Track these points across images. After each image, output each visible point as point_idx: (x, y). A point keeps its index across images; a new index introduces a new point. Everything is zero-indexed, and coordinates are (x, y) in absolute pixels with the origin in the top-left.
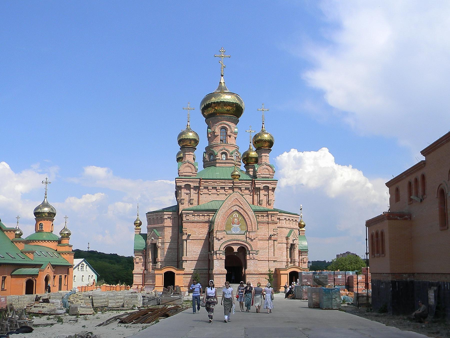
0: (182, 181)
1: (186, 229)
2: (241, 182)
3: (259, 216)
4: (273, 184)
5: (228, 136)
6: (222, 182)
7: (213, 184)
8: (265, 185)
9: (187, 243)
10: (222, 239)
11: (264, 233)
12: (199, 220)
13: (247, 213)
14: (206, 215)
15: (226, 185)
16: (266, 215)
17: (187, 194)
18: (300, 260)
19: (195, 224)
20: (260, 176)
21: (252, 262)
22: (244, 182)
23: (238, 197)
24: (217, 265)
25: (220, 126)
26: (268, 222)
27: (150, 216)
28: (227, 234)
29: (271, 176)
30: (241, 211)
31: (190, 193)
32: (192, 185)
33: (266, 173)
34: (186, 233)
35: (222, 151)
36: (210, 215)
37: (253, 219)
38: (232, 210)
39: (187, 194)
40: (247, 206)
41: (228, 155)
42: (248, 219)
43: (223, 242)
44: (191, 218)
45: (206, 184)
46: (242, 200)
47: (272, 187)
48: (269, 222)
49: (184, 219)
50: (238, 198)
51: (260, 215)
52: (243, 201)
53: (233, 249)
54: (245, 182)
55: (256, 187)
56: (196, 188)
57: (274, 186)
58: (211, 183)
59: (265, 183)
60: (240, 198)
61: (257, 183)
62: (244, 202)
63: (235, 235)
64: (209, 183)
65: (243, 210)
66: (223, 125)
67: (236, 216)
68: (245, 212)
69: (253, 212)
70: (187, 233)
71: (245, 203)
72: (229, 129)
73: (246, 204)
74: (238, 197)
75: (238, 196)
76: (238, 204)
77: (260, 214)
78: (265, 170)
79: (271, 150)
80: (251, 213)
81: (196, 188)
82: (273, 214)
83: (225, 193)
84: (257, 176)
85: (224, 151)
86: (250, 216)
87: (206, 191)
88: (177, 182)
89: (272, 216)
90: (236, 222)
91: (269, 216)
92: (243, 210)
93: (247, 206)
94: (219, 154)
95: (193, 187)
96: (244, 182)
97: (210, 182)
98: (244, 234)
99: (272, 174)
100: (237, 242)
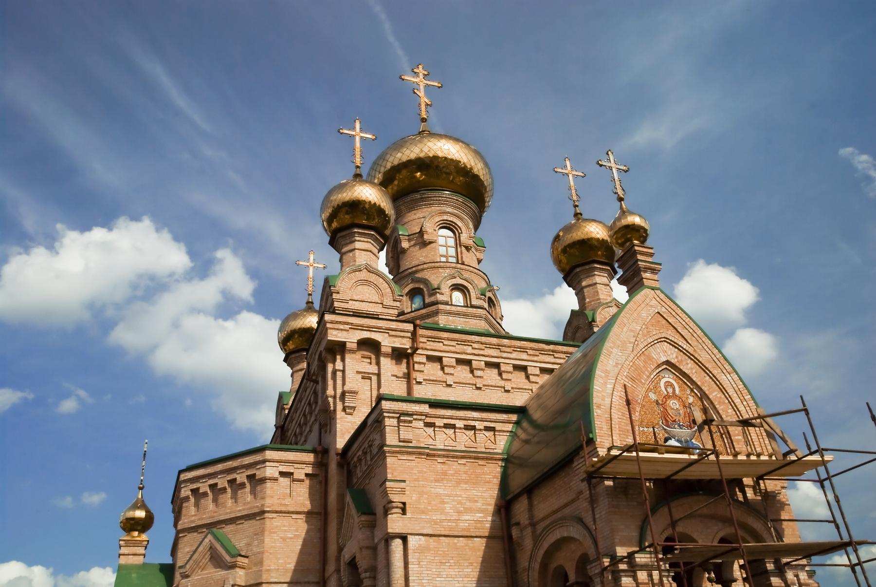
0: (348, 324)
2: (553, 351)
5: (464, 246)
6: (491, 346)
7: (459, 348)
13: (714, 378)
14: (482, 428)
15: (505, 355)
17: (366, 376)
19: (439, 466)
25: (437, 219)
30: (688, 367)
31: (379, 375)
32: (387, 343)
34: (401, 505)
35: (455, 281)
36: (498, 426)
37: (745, 403)
38: (650, 358)
39: (366, 376)
40: (706, 347)
41: (473, 295)
42: (724, 403)
44: (418, 434)
45: (433, 348)
46: (684, 323)
49: (391, 439)
52: (687, 327)
56: (399, 355)
58: (454, 343)
60: (674, 313)
64: (446, 342)
66: (445, 217)
67: (670, 390)
70: (404, 504)
73: (700, 341)
74: (664, 309)
76: (671, 334)
80: (730, 378)
81: (399, 355)
83: (502, 383)
85: (458, 281)
87: (432, 370)
88: (331, 328)
90: (680, 419)
93: (706, 347)
94: (445, 289)
95: (390, 350)
97: (448, 339)
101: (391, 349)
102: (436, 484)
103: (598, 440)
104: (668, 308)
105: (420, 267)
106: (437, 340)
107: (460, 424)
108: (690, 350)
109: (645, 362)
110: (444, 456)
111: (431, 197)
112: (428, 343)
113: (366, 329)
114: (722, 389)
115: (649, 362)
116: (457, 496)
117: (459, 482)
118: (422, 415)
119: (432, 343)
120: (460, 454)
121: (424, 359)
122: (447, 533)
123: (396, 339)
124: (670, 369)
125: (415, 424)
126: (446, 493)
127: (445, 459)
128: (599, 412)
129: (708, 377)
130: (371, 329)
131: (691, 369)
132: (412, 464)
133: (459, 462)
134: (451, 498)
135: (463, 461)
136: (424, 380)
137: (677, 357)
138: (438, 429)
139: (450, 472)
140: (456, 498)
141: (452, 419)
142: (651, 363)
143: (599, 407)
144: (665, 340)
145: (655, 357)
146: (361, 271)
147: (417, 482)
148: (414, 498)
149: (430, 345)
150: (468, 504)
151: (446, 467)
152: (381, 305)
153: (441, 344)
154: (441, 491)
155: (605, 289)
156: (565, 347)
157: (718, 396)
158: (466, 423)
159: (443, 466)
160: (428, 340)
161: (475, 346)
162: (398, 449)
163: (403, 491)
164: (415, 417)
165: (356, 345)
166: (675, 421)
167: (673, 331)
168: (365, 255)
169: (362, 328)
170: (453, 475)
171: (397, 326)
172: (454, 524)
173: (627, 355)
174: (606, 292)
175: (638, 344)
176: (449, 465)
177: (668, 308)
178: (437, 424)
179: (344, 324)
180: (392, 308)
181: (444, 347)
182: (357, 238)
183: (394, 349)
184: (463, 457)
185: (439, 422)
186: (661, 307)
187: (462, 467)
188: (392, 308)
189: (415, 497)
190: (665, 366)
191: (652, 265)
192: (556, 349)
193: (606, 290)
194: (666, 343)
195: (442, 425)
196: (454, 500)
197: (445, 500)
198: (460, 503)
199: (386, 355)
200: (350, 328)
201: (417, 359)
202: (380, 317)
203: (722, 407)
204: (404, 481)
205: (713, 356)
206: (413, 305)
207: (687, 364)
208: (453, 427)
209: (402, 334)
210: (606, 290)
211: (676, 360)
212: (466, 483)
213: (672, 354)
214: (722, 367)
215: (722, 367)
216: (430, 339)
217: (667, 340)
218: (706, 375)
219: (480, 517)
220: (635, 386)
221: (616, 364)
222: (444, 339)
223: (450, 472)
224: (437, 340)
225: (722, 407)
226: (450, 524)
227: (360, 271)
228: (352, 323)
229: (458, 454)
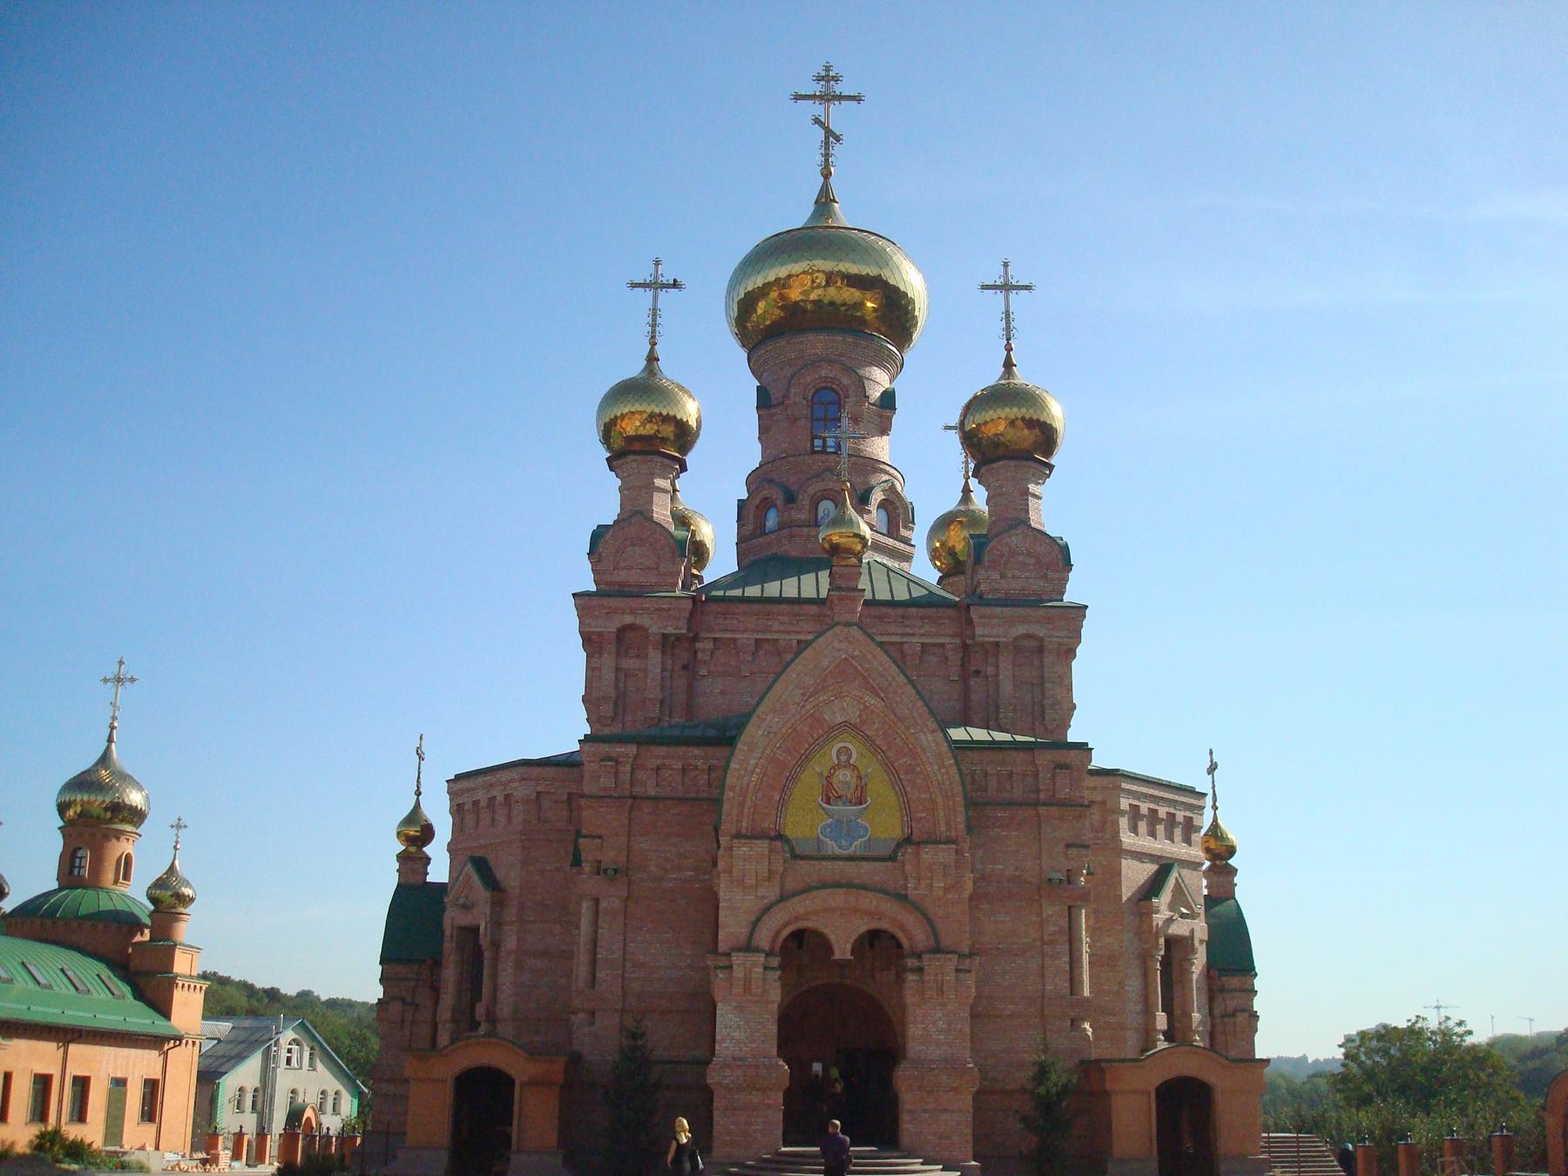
1: (598, 841)
9: (601, 915)
11: (1016, 869)
18: (1218, 1021)
21: (934, 1023)
24: (736, 1034)
27: (463, 791)
31: (645, 670)
53: (824, 945)
66: (824, 372)
67: (843, 758)
79: (1051, 467)
98: (892, 858)
103: (722, 827)
128: (732, 794)
137: (860, 716)
157: (909, 762)
161: (786, 619)
166: (840, 797)
175: (803, 706)
203: (909, 777)
204: (600, 837)
207: (874, 723)
219: (691, 876)
225: (909, 777)
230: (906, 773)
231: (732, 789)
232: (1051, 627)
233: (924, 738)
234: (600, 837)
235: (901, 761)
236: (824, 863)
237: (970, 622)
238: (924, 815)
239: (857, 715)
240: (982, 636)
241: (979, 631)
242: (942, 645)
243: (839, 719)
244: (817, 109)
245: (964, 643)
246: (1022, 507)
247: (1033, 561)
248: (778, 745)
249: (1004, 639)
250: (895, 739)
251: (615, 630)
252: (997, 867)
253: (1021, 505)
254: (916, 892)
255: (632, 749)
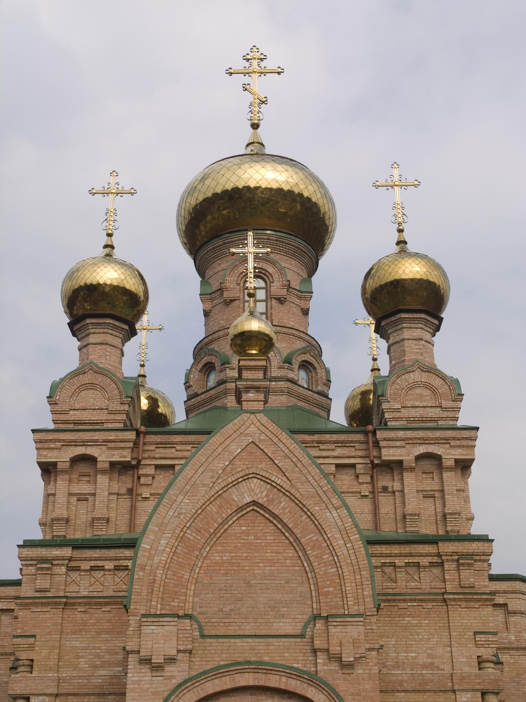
0: (59, 441)
1: (32, 640)
2: (319, 442)
3: (394, 565)
4: (458, 443)
5: (275, 299)
8: (422, 449)
10: (171, 660)
11: (429, 656)
12: (100, 594)
13: (312, 517)
16: (430, 559)
20: (398, 415)
22: (330, 442)
23: (263, 437)
26: (443, 594)
28: (203, 636)
29: (445, 414)
33: (424, 404)
34: (28, 663)
39: (82, 498)
42: (320, 547)
43: (175, 682)
45: (163, 456)
47: (457, 457)
48: (446, 596)
50: (261, 441)
51: (398, 562)
52: (291, 455)
54: (335, 442)
55: (384, 458)
57: (462, 455)
58: (188, 447)
59: (425, 441)
60: (276, 440)
61: (385, 440)
62: (295, 460)
63: (250, 640)
64: (179, 447)
65: (292, 498)
68: (302, 507)
69: (359, 545)
70: (32, 660)
71: (299, 465)
72: (276, 276)
75: (262, 428)
76: (262, 467)
77: (400, 555)
78: (418, 391)
82: (462, 555)
84: (387, 416)
86: (333, 533)
89: (463, 564)
91: (447, 566)
92: (292, 498)
95: (107, 465)
96: (330, 442)
97: (182, 443)
98: (302, 636)
99: (450, 404)
100: (260, 680)
101: (108, 464)
102: (73, 636)
103: (132, 607)
104: (268, 433)
105: (216, 335)
106: (168, 446)
107: (110, 565)
108: (287, 486)
109: (220, 507)
110: (85, 604)
111: (235, 241)
112: (158, 451)
113: (81, 444)
114: (320, 530)
115: (225, 507)
116: (94, 648)
117: (99, 633)
118: (64, 560)
119: (162, 450)
120: (103, 600)
121: (151, 471)
122: (76, 691)
123: (116, 452)
124: (258, 510)
125: (56, 570)
126: (83, 645)
127: (87, 607)
128: (142, 574)
129: (306, 516)
130: (86, 444)
131: (284, 508)
132: (46, 616)
133: (103, 610)
134: (87, 651)
135: (108, 608)
136: (151, 494)
137: (267, 496)
138: (83, 574)
139: (91, 621)
140: (93, 651)
141: (101, 560)
142: (229, 507)
143: (143, 568)
144: (254, 475)
145: (236, 498)
146: (86, 373)
147: (49, 636)
148: (43, 654)
149: (160, 453)
150: (107, 657)
151: (88, 615)
152: (106, 412)
153: (173, 450)
154: (77, 644)
155: (416, 345)
156: (334, 435)
157: (314, 538)
158: (116, 563)
159: (84, 615)
160: (156, 447)
162: (30, 601)
163: (31, 647)
164: (56, 562)
165: (68, 464)
167: (268, 463)
168: (100, 349)
169: (75, 443)
170: (94, 625)
171: (116, 436)
172: (86, 681)
173: (196, 501)
174: (417, 349)
175: (213, 487)
176: (90, 613)
177: (268, 433)
178: (82, 568)
179: (55, 442)
180: (119, 412)
181: (177, 453)
182: (92, 331)
183: (112, 464)
184: (106, 604)
185: (85, 566)
186: (260, 434)
187: (106, 615)
188: (119, 412)
189: (44, 653)
190: (251, 508)
191: (255, 383)
192: (322, 439)
193: (417, 347)
194: (255, 480)
195: (89, 568)
196: (90, 654)
197: (80, 654)
198: (98, 656)
199: (103, 472)
200: (62, 445)
201: (141, 472)
202: (106, 426)
204: (34, 636)
205: (318, 489)
206: (208, 383)
207: (281, 502)
208: (101, 568)
209: (122, 445)
210: (417, 347)
211: (265, 499)
212: (108, 633)
213: (262, 492)
214: (327, 502)
215: (327, 502)
216: (160, 446)
217: (257, 476)
218: (303, 514)
219: (119, 672)
220: (199, 538)
221: (178, 514)
222: (176, 444)
223: (91, 621)
224: (168, 446)
226: (80, 681)
227: (84, 373)
228: (64, 440)
229: (101, 600)
230: (313, 548)
231: (143, 568)
232: (447, 446)
233: (329, 514)
234: (34, 636)
235: (307, 538)
236: (233, 640)
237: (376, 444)
238: (331, 589)
239: (264, 494)
240: (386, 456)
241: (384, 452)
242: (353, 466)
243: (248, 500)
244: (246, 79)
245: (372, 462)
246: (418, 351)
247: (429, 392)
248: (187, 526)
249: (407, 458)
250: (302, 516)
251: (68, 460)
252: (410, 654)
253: (417, 349)
254: (326, 668)
255: (67, 552)
